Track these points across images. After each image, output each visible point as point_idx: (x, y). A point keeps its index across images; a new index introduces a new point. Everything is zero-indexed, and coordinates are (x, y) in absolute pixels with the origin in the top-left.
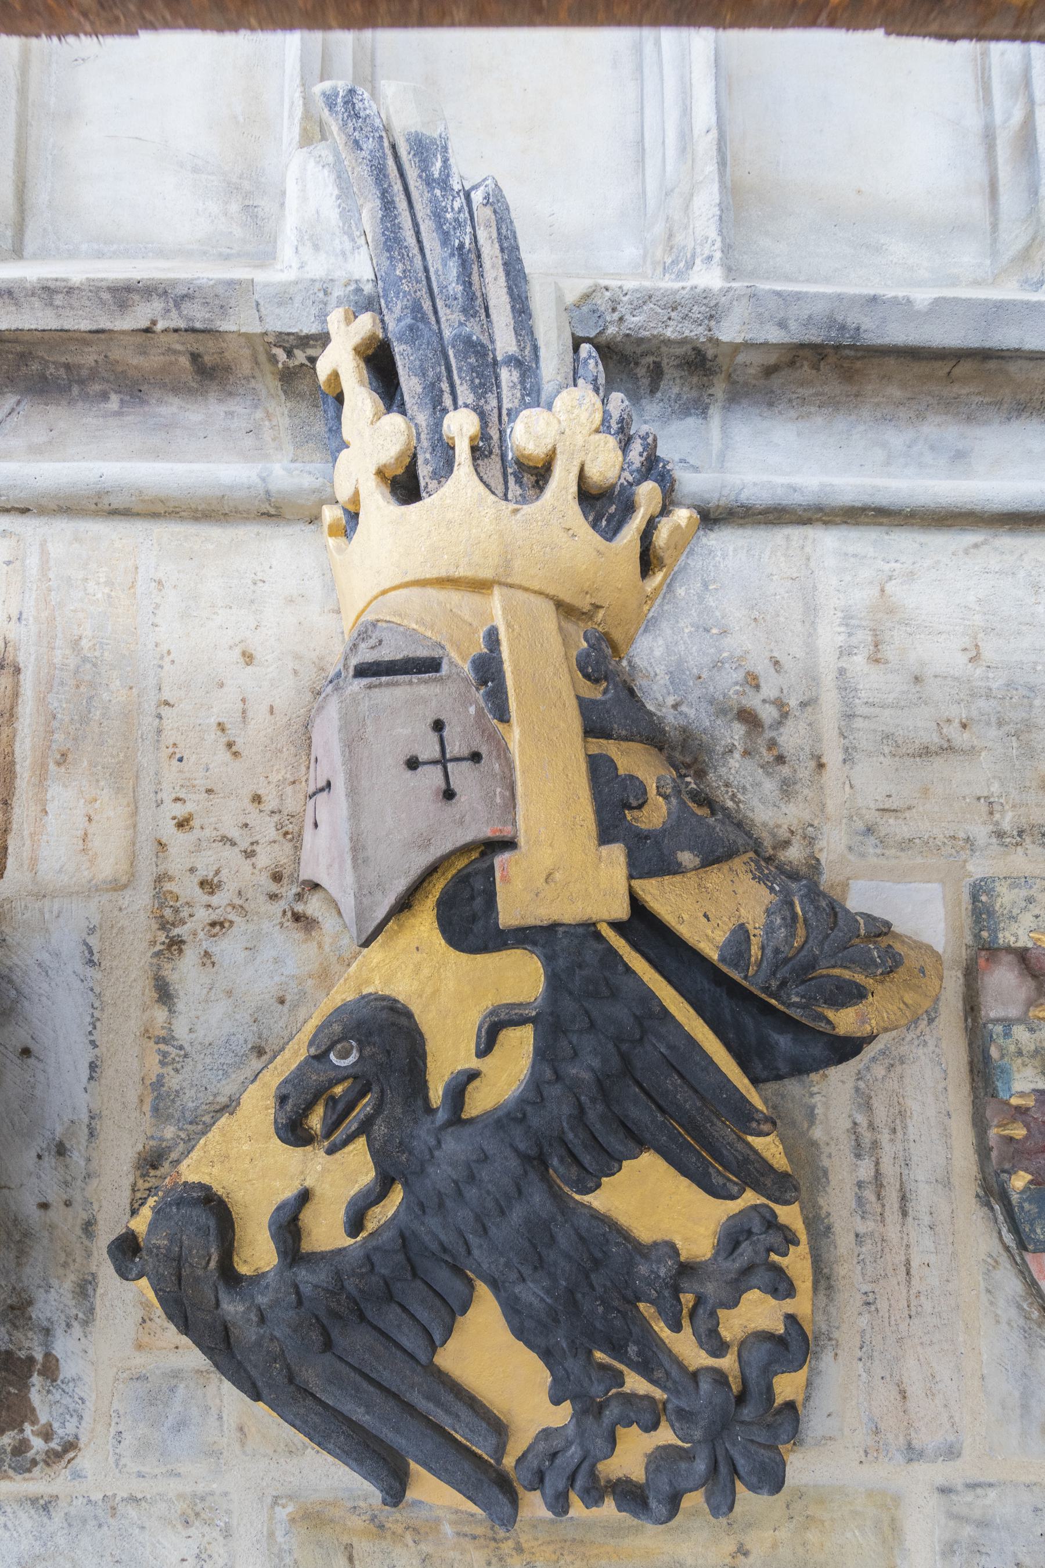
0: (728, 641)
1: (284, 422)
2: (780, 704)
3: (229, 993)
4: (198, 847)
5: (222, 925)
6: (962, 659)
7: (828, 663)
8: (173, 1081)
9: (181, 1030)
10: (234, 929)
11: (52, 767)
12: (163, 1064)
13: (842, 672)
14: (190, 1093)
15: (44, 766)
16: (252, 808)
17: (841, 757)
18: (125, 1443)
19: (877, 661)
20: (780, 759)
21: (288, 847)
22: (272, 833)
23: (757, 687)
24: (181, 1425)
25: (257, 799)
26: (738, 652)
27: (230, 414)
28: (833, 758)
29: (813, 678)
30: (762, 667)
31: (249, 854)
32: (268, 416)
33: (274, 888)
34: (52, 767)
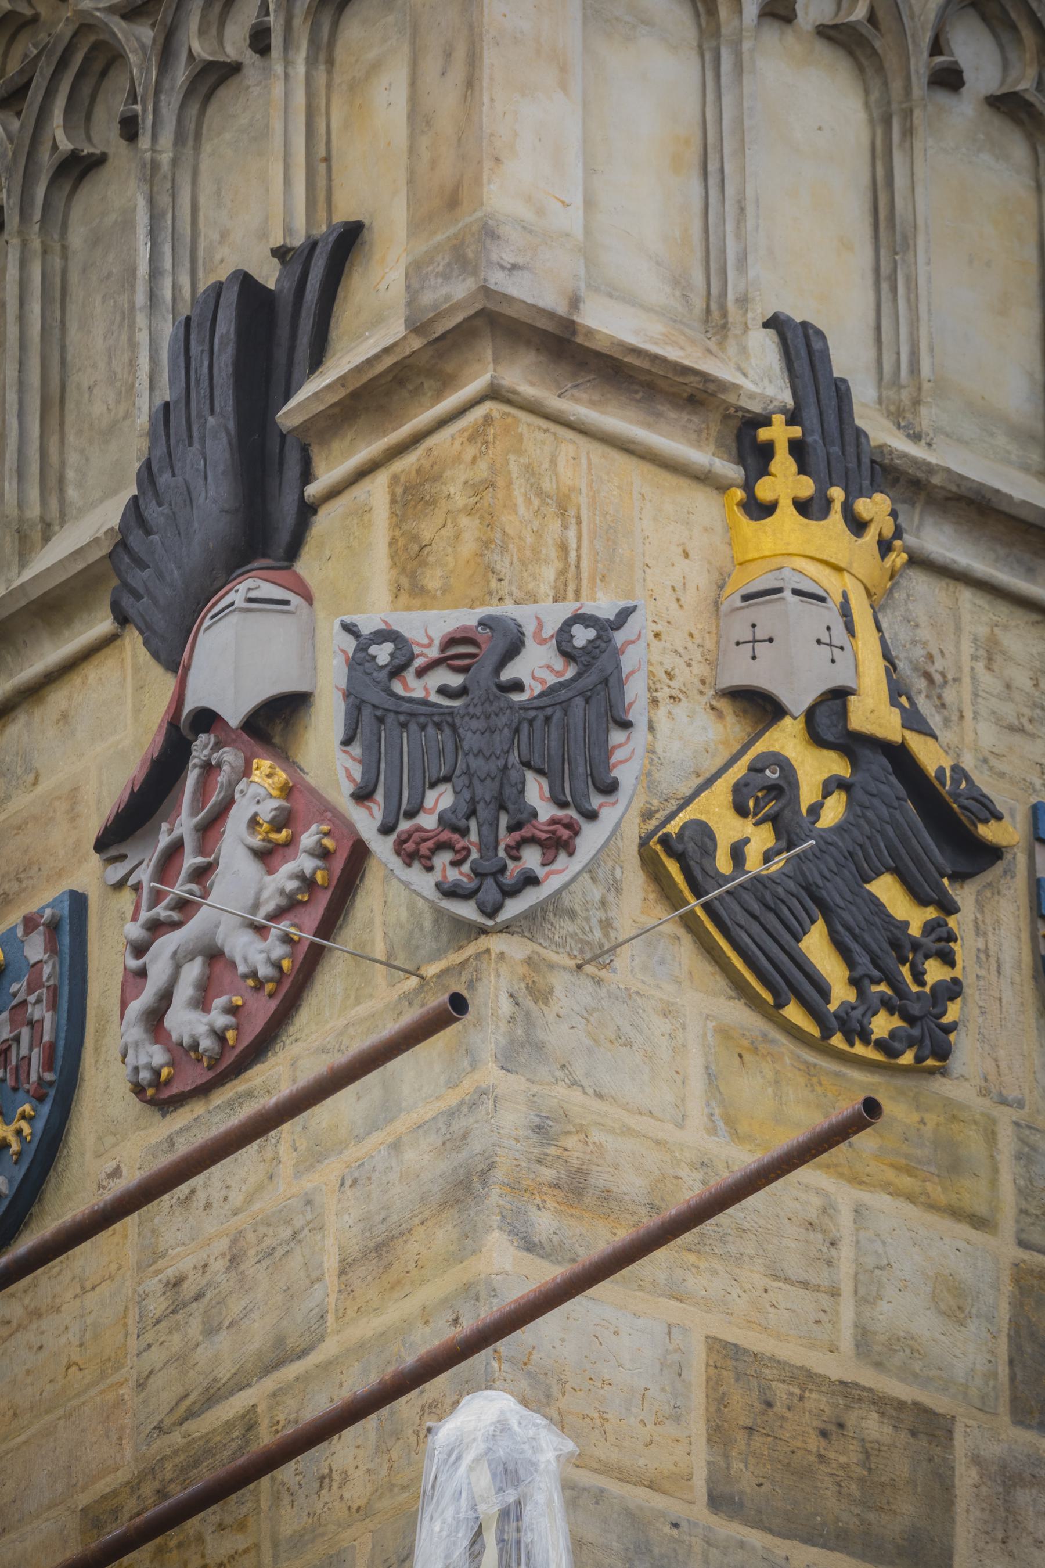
0: (918, 631)
1: (714, 433)
2: (943, 675)
3: (681, 738)
4: (664, 651)
5: (674, 698)
6: (1030, 683)
7: (966, 663)
8: (657, 776)
9: (659, 750)
10: (681, 704)
11: (598, 581)
12: (651, 764)
13: (972, 669)
14: (665, 785)
15: (594, 579)
16: (688, 639)
17: (972, 716)
18: (636, 962)
19: (989, 669)
20: (943, 706)
21: (708, 667)
22: (700, 658)
23: (933, 662)
24: (662, 962)
25: (691, 635)
26: (924, 639)
27: (690, 421)
28: (968, 714)
29: (960, 669)
30: (935, 652)
31: (689, 665)
32: (708, 428)
33: (701, 687)
34: (598, 581)
